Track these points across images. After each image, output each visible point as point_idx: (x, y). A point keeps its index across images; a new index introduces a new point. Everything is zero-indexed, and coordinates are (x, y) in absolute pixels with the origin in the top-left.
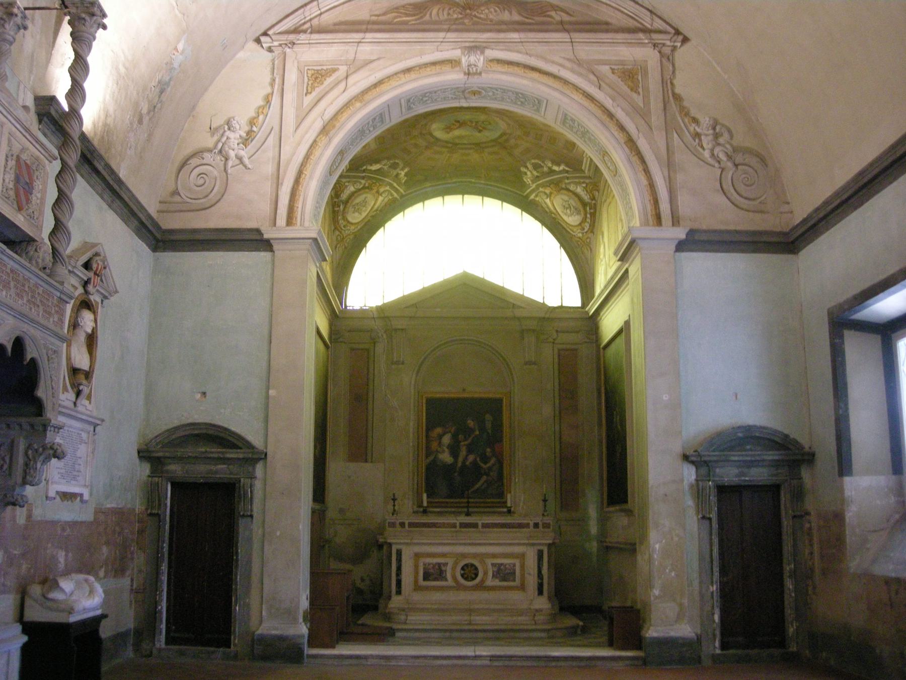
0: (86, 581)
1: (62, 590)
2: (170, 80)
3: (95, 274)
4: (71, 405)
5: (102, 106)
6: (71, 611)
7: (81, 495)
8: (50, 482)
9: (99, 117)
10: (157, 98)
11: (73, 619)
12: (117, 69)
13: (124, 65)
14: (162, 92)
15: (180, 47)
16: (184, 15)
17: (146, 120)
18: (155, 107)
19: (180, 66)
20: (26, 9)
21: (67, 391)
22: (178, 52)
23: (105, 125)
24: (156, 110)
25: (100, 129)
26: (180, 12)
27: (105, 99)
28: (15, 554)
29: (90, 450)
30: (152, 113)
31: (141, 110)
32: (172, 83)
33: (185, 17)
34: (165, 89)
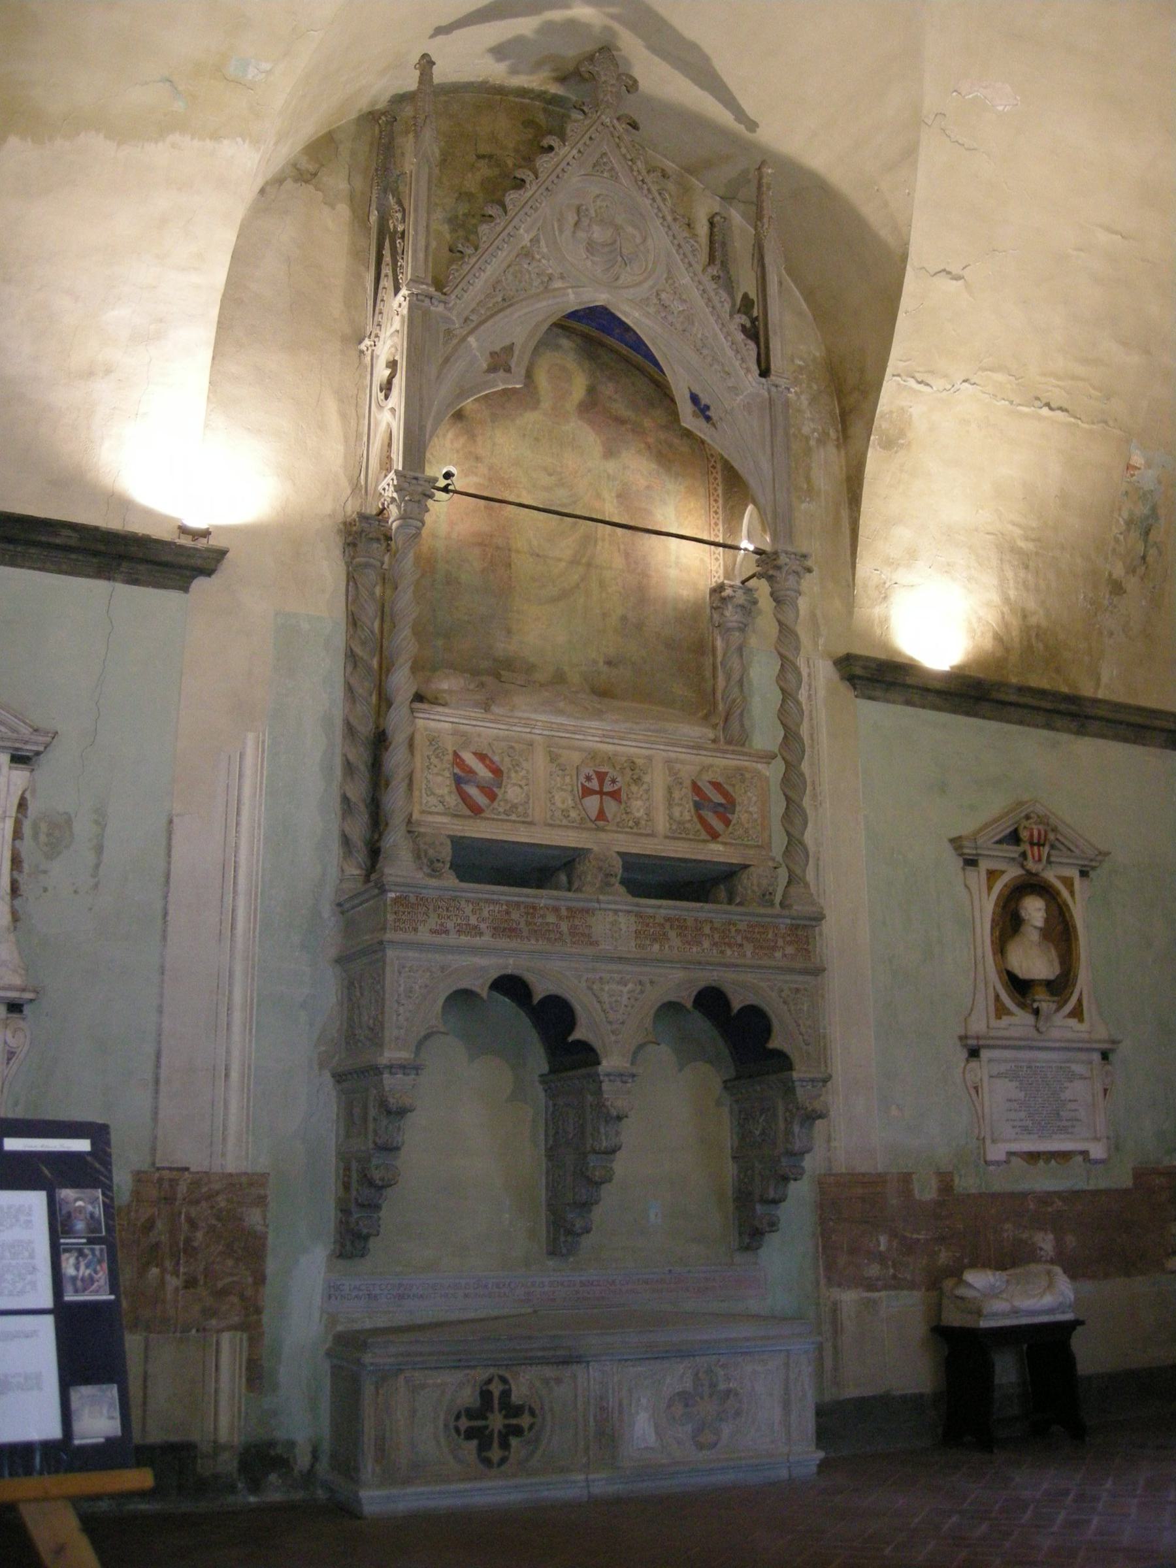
0: (1049, 1273)
1: (970, 1286)
2: (1154, 509)
3: (1032, 844)
4: (1033, 1033)
5: (1006, 609)
6: (979, 1313)
7: (1084, 1153)
8: (988, 1142)
9: (1006, 625)
10: (1140, 547)
11: (984, 1324)
12: (1015, 550)
13: (1027, 539)
14: (1147, 533)
15: (1138, 459)
16: (1106, 422)
17: (1132, 584)
18: (1144, 558)
19: (1160, 482)
20: (743, 582)
21: (1009, 1013)
22: (1139, 469)
23: (1026, 630)
24: (1150, 559)
25: (1017, 640)
26: (1093, 423)
27: (1006, 600)
28: (919, 1240)
29: (1099, 1088)
30: (1143, 568)
31: (1110, 575)
32: (1162, 512)
33: (1111, 423)
34: (1151, 525)
